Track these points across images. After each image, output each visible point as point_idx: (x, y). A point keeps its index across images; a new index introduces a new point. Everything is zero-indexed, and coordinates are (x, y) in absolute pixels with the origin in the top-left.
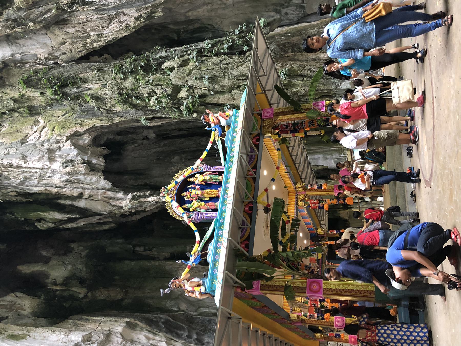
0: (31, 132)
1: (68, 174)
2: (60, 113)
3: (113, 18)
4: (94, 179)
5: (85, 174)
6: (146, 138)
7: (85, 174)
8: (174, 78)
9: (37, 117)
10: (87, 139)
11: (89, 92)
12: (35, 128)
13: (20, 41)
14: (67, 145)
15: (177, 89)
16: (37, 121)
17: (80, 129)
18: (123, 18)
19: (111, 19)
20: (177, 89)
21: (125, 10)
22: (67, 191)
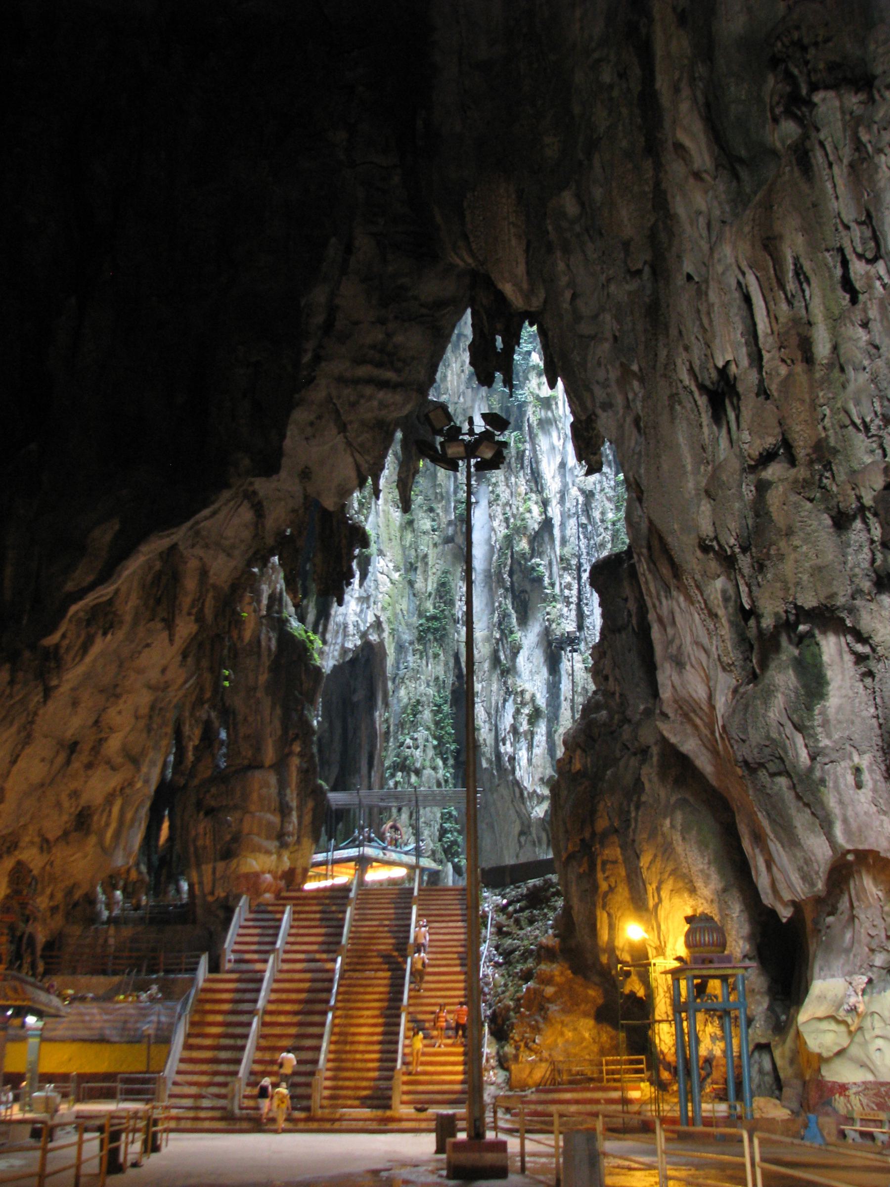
0: (387, 559)
1: (346, 626)
2: (404, 606)
3: (490, 719)
4: (336, 654)
5: (343, 647)
6: (355, 691)
7: (343, 647)
8: (428, 772)
9: (402, 572)
10: (373, 637)
11: (424, 662)
12: (391, 565)
13: (486, 590)
14: (371, 619)
15: (418, 772)
16: (397, 569)
17: (386, 635)
18: (487, 726)
19: (489, 714)
20: (418, 772)
21: (493, 733)
22: (331, 626)
